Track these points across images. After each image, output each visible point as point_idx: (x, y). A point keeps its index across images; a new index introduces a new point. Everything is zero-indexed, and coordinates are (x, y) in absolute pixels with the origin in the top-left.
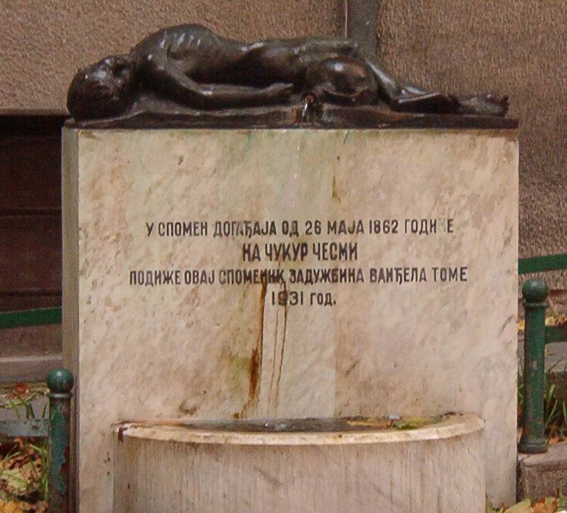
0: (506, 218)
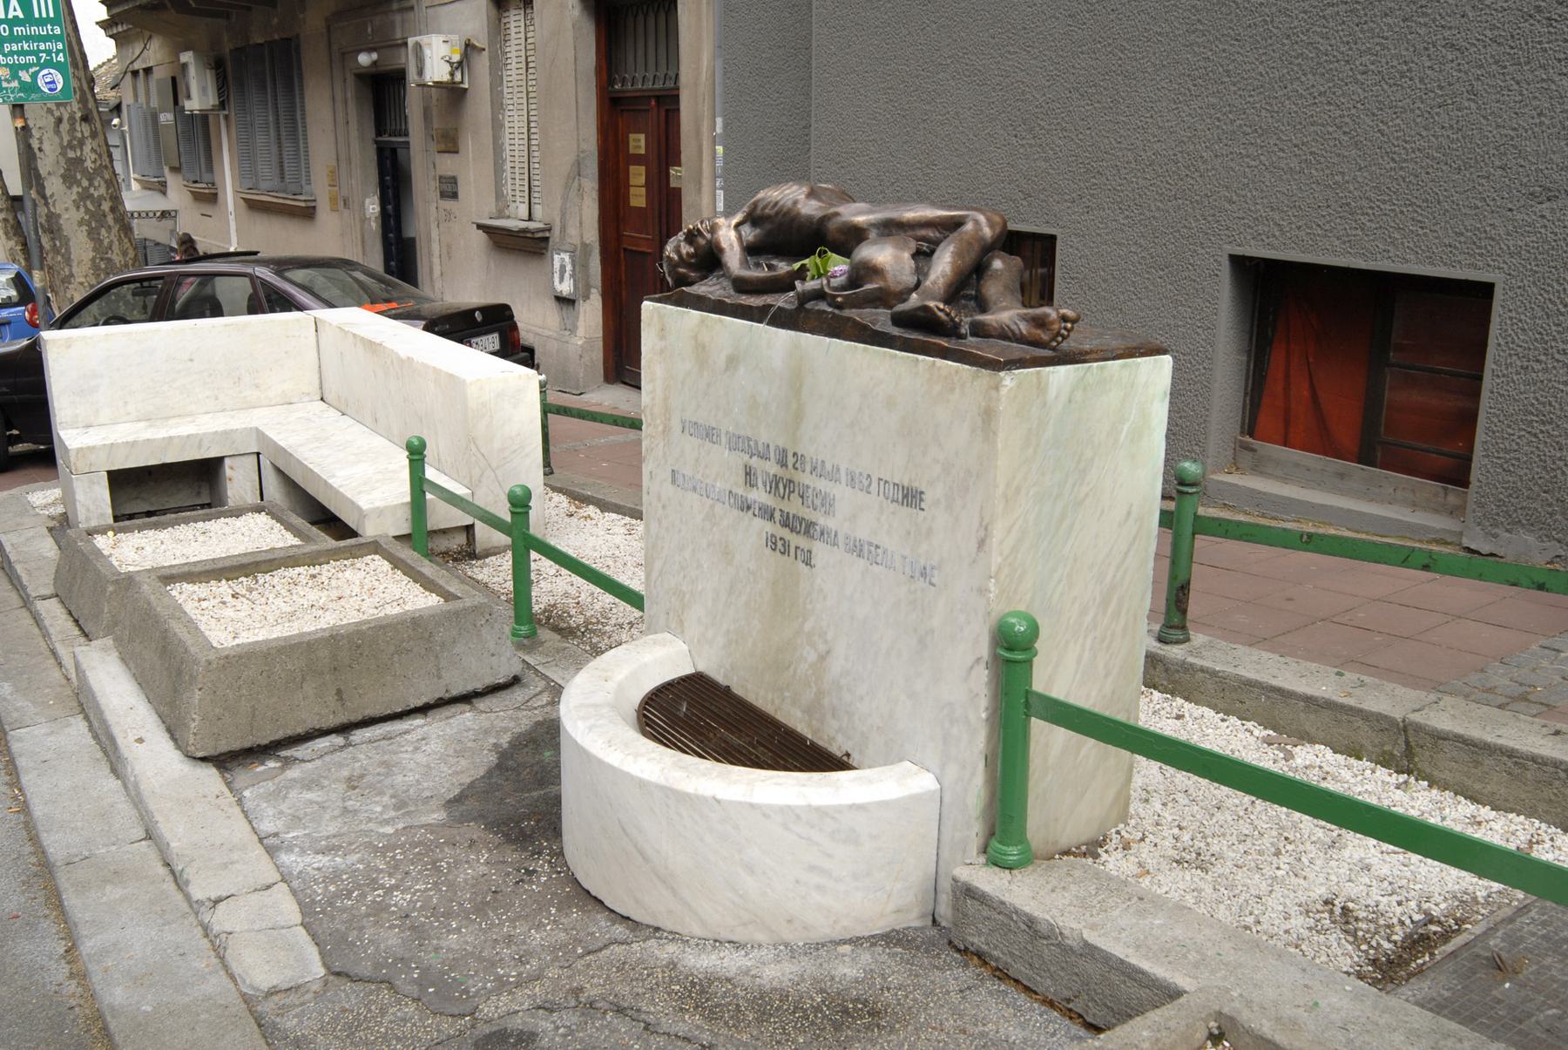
0: (982, 507)
